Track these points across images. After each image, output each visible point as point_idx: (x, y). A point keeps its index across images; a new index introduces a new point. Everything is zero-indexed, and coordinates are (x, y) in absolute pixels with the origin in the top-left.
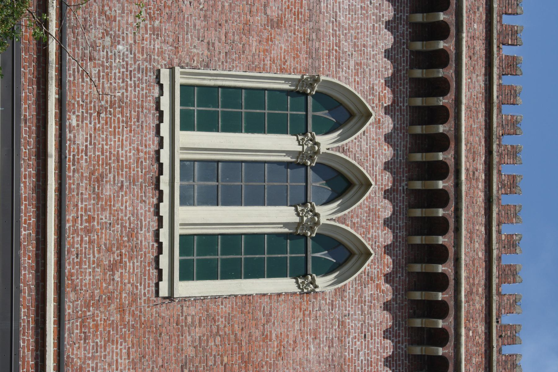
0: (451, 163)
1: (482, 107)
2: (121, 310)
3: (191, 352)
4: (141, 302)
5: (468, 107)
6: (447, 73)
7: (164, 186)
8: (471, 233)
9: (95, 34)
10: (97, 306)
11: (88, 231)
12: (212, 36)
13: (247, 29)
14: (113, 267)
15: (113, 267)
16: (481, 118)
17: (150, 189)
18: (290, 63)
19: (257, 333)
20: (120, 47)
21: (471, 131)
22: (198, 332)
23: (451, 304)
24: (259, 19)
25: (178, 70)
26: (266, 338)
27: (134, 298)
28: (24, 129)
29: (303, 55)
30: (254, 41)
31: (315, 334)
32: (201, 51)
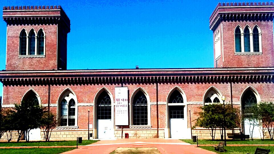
0: (29, 17)
1: (22, 12)
2: (46, 62)
3: (51, 53)
4: (45, 59)
5: (22, 15)
6: (17, 18)
7: (32, 57)
8: (38, 14)
9: (15, 66)
10: (45, 65)
11: (37, 66)
12: (15, 51)
13: (14, 46)
14: (41, 63)
15: (41, 63)
16: (23, 12)
17: (33, 59)
18: (18, 40)
19: (50, 44)
20: (17, 62)
21: (25, 14)
22: (49, 52)
23: (47, 17)
24: (13, 45)
25: (19, 56)
26: (51, 43)
27: (45, 60)
28: (25, 75)
29: (17, 39)
30: (15, 45)
31: (51, 36)
32: (17, 53)
